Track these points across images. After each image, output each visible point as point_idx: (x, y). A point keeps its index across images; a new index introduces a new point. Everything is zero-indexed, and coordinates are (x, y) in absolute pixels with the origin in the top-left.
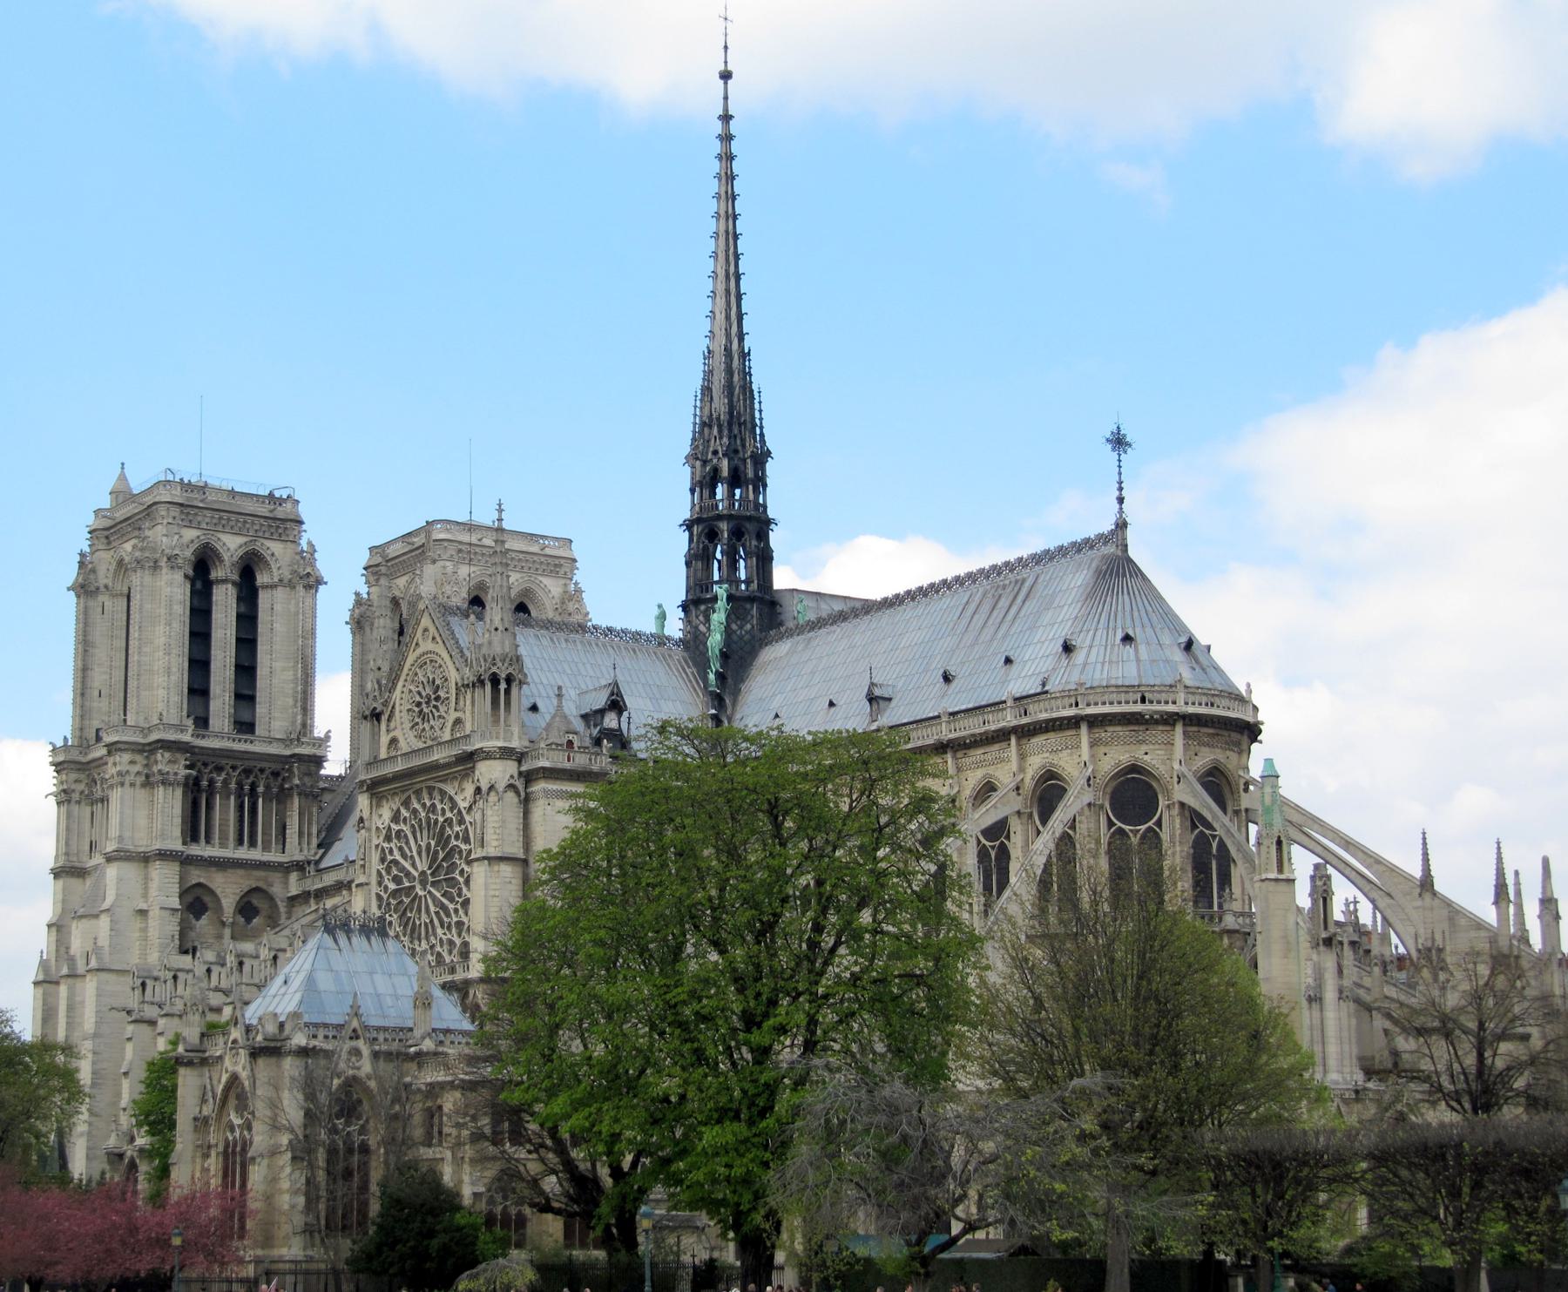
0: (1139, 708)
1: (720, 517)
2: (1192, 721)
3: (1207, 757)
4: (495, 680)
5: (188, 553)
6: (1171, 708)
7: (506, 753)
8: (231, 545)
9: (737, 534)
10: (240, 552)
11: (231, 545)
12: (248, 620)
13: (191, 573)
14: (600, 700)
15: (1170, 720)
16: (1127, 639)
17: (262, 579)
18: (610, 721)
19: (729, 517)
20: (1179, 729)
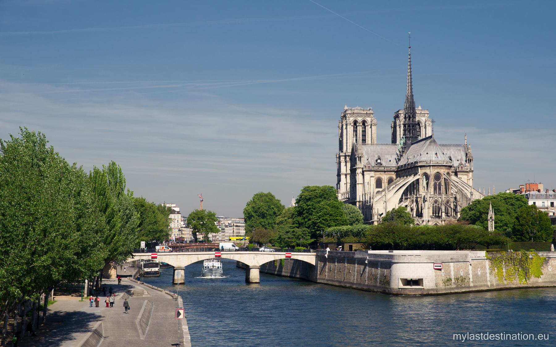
0: (425, 164)
1: (406, 124)
2: (433, 166)
3: (436, 171)
4: (358, 157)
5: (352, 122)
6: (430, 164)
7: (359, 168)
8: (360, 119)
9: (409, 126)
10: (361, 120)
11: (360, 119)
12: (364, 132)
13: (353, 124)
14: (376, 158)
15: (430, 166)
16: (427, 153)
17: (366, 124)
18: (379, 161)
19: (407, 124)
20: (431, 167)
